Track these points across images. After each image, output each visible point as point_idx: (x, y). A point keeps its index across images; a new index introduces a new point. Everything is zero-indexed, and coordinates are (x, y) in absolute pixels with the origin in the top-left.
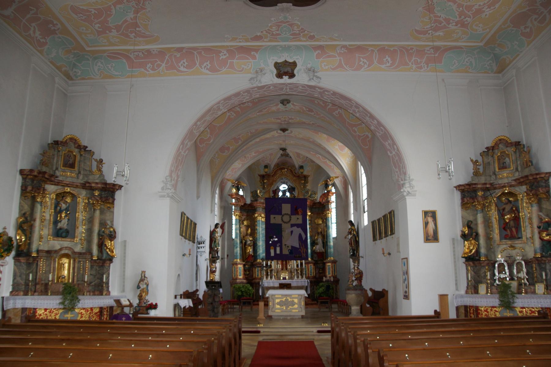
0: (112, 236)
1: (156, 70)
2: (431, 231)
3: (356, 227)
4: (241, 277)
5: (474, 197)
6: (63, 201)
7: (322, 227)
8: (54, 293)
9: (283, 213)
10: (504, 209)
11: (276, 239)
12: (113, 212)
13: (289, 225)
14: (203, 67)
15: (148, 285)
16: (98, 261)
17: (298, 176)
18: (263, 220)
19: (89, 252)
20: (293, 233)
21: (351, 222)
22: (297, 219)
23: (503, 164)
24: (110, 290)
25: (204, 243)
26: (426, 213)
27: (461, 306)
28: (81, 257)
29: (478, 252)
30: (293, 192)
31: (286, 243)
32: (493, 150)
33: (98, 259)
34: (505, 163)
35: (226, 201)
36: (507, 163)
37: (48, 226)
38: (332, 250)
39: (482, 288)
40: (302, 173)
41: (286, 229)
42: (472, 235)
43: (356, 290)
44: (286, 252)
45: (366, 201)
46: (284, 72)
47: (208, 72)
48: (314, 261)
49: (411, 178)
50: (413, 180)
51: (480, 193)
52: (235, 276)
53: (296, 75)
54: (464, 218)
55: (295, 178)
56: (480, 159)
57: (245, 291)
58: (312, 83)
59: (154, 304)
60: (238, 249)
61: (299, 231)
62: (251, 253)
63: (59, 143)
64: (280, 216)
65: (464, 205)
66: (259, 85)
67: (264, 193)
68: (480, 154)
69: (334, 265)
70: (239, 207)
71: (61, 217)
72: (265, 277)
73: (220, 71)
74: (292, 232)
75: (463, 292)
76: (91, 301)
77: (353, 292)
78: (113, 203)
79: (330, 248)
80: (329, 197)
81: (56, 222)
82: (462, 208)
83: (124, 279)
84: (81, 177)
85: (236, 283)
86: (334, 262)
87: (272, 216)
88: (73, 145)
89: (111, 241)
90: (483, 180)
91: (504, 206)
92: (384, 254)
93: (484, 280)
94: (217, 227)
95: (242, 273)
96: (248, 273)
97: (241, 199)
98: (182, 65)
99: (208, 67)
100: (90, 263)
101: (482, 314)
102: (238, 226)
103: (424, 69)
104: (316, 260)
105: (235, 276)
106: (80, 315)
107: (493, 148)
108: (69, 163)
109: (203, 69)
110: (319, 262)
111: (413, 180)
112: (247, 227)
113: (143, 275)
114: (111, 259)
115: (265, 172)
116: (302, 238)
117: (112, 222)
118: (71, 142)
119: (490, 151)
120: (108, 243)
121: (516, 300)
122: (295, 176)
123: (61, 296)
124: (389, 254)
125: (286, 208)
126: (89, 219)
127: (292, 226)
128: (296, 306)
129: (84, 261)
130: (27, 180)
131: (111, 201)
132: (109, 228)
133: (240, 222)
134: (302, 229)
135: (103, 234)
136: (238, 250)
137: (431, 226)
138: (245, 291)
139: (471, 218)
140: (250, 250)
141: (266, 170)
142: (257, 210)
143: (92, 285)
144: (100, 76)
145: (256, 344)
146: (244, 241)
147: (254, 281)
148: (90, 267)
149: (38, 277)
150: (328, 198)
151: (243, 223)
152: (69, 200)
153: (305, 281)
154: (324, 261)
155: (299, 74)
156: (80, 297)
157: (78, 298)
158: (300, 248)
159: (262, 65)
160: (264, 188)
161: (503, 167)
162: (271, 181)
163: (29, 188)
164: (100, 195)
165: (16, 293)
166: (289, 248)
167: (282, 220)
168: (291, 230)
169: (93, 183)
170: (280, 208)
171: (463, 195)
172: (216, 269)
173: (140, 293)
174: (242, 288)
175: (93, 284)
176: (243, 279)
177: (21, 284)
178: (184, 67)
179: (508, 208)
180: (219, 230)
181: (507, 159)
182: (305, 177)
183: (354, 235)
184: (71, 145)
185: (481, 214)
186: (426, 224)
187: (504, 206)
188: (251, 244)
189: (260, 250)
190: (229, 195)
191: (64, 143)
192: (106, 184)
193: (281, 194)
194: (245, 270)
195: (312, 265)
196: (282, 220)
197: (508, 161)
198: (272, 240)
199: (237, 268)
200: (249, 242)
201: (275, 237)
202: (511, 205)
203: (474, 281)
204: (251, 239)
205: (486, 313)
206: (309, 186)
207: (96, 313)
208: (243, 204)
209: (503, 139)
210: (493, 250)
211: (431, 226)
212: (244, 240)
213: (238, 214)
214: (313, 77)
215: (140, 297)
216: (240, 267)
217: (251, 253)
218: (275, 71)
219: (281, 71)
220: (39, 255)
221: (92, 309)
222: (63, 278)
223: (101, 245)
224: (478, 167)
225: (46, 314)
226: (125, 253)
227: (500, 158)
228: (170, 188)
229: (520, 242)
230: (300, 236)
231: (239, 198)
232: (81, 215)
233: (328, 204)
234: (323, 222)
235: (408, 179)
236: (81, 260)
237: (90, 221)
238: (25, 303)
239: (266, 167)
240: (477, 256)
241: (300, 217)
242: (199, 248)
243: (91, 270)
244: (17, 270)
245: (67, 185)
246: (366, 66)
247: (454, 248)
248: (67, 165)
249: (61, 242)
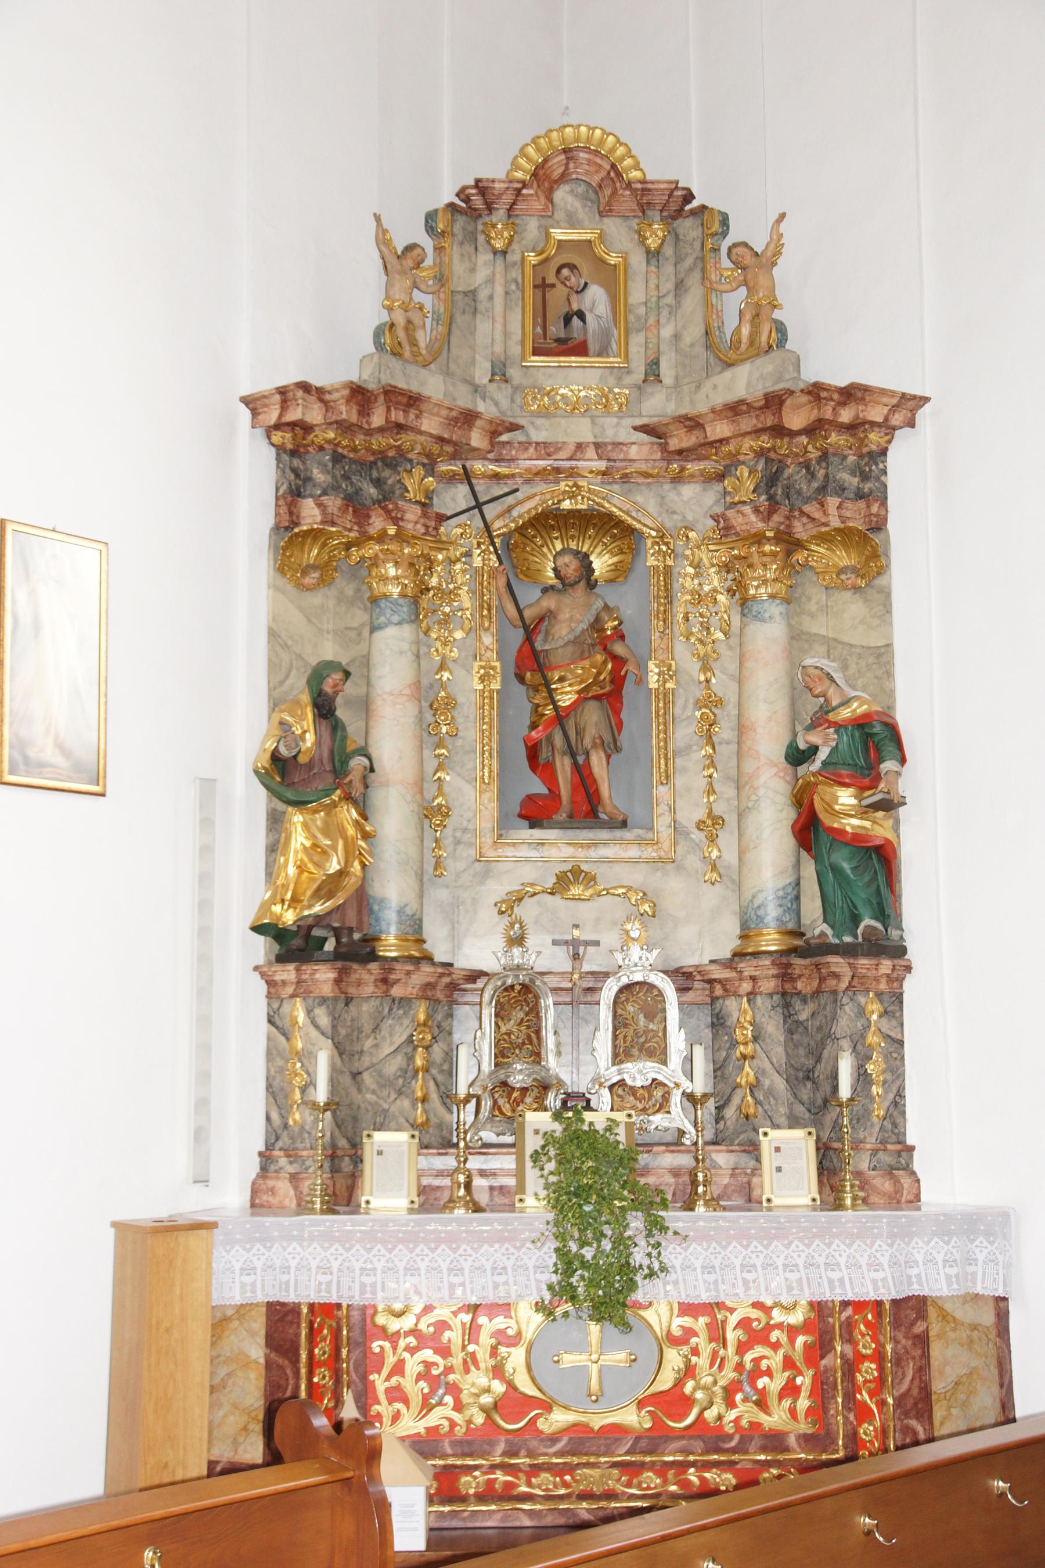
23: (567, 320)
34: (581, 315)
36: (589, 317)
54: (285, 646)
68: (430, 218)
91: (550, 602)
121: (672, 1253)
171: (295, 471)
185: (407, 632)
202: (610, 595)
205: (428, 1354)
227: (551, 279)
229: (633, 852)
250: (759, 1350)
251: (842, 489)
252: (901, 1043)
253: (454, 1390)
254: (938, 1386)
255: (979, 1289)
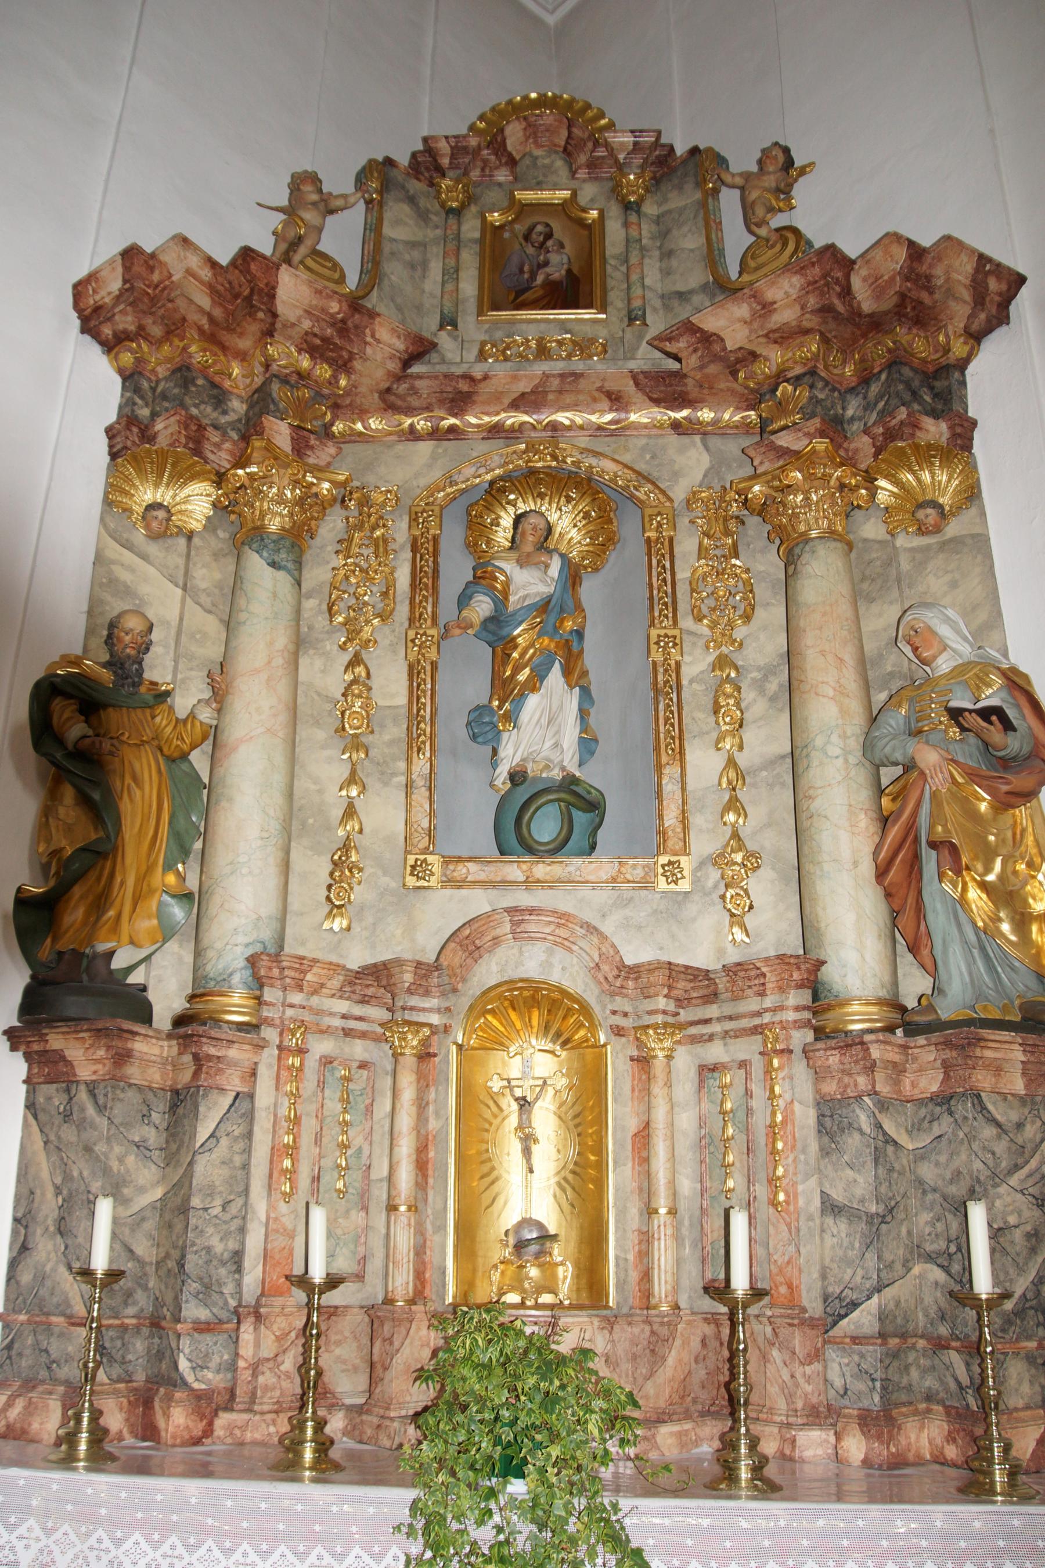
12: (980, 544)
28: (716, 1028)
37: (402, 765)
88: (559, 163)
108: (540, 279)
220: (266, 1012)
236: (716, 1052)
243: (825, 1152)
244: (44, 1168)
248: (528, 296)
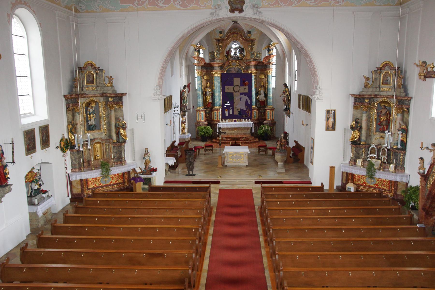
0: (124, 128)
1: (141, 5)
2: (330, 124)
3: (289, 88)
4: (203, 120)
5: (362, 102)
6: (90, 107)
7: (265, 81)
8: (96, 168)
9: (234, 84)
10: (381, 112)
11: (230, 104)
12: (123, 111)
13: (239, 93)
14: (176, 3)
15: (150, 157)
16: (117, 144)
17: (247, 40)
18: (219, 75)
19: (110, 137)
20: (241, 100)
21: (285, 85)
22: (244, 89)
23: (386, 81)
24: (126, 160)
25: (178, 108)
26: (328, 112)
27: (345, 172)
29: (360, 138)
30: (242, 52)
31: (236, 107)
32: (381, 70)
33: (117, 142)
34: (387, 80)
35: (190, 61)
38: (271, 100)
39: (359, 162)
40: (250, 37)
41: (237, 97)
42: (357, 128)
43: (281, 153)
44: (236, 113)
45: (297, 72)
46: (235, 8)
47: (180, 7)
48: (258, 107)
49: (320, 88)
50: (322, 89)
51: (367, 101)
52: (199, 119)
53: (244, 10)
54: (354, 115)
55: (244, 41)
56: (371, 77)
57: (207, 131)
58: (255, 17)
59: (155, 168)
60: (201, 99)
61: (246, 97)
62: (210, 101)
63: (82, 68)
64: (232, 87)
65: (356, 107)
66: (218, 18)
67: (220, 54)
68: (372, 71)
69: (272, 112)
70: (200, 66)
71: (90, 117)
72: (221, 120)
73: (188, 6)
74: (241, 99)
75: (347, 161)
76: (117, 170)
77: (279, 154)
78: (122, 105)
79: (270, 99)
80: (270, 59)
81: (88, 121)
82: (354, 109)
83: (134, 153)
84: (99, 89)
85: (200, 125)
86: (272, 109)
87: (226, 87)
89: (124, 130)
90: (369, 92)
92: (303, 124)
93: (360, 157)
94: (185, 88)
95: (204, 117)
96: (208, 116)
97: (201, 60)
98: (160, 2)
99: (180, 4)
100: (112, 145)
101: (356, 178)
102: (200, 82)
103: (340, 4)
104: (259, 106)
105: (199, 119)
106: (112, 178)
107: (381, 69)
109: (176, 4)
110: (261, 108)
111: (322, 89)
112: (207, 81)
113: (146, 151)
114: (125, 142)
115: (221, 37)
116: (248, 103)
117: (123, 117)
118: (89, 66)
119: (379, 70)
120: (122, 131)
122: (244, 39)
123: (100, 170)
124: (307, 125)
125: (237, 81)
126: (107, 116)
127: (241, 94)
128: (242, 159)
129: (108, 144)
130: (68, 100)
131: (121, 103)
132: (122, 122)
133: (202, 77)
134: (248, 96)
135: (118, 126)
136: (200, 100)
137: (331, 120)
138: (207, 131)
139: (359, 116)
140: (209, 99)
141: (221, 35)
142: (214, 68)
143: (116, 159)
144: (100, 10)
145: (218, 192)
146: (204, 92)
147: (213, 122)
148: (112, 147)
149: (84, 159)
150: (269, 60)
151: (203, 78)
152: (93, 105)
153: (250, 124)
154: (265, 108)
155: (246, 9)
156: (111, 168)
157: (110, 170)
158: (246, 110)
159: (220, 3)
160: (219, 50)
161: (386, 83)
162: (225, 44)
163: (71, 105)
164: (113, 101)
165: (75, 170)
166: (238, 110)
167: (234, 90)
168: (240, 97)
169: (108, 94)
170: (232, 81)
171: (356, 100)
172: (186, 120)
173: (145, 162)
174: (204, 130)
175: (116, 157)
176: (205, 121)
177: (76, 164)
178: (162, 3)
179: (384, 111)
180: (186, 90)
181: (389, 78)
182: (252, 41)
183: (287, 95)
184: (90, 67)
186: (328, 119)
187: (382, 110)
188: (210, 95)
189: (217, 99)
190: (192, 57)
191: (85, 68)
192: (117, 94)
193: (233, 52)
194: (206, 114)
195: (256, 110)
196: (234, 90)
197: (390, 79)
198: (226, 105)
199: (200, 114)
200: (208, 93)
201: (228, 102)
202: (386, 110)
203: (355, 157)
204: (210, 90)
205: (358, 178)
206: (255, 48)
207: (120, 176)
208: (203, 64)
209: (389, 64)
210: (370, 137)
211: (331, 120)
212: (204, 91)
213: (200, 72)
214: (257, 12)
215: (146, 164)
216: (203, 113)
217: (210, 101)
218: (229, 7)
219: (233, 7)
221: (118, 174)
222: (98, 156)
223: (118, 133)
224: (368, 82)
225: (93, 181)
226: (133, 137)
227: (385, 76)
228: (159, 94)
230: (247, 101)
231: (200, 60)
232: (103, 115)
233: (270, 65)
234: (265, 77)
235: (319, 88)
236: (106, 143)
237: (108, 117)
238: (82, 176)
239: (221, 32)
240: (359, 141)
241: (247, 88)
242: (174, 111)
244: (73, 157)
245: (92, 97)
246: (296, 3)
247: (345, 135)
249: (93, 134)
250: (385, 183)
251: (406, 103)
252: (405, 158)
253: (360, 181)
254: (398, 188)
255: (404, 181)
